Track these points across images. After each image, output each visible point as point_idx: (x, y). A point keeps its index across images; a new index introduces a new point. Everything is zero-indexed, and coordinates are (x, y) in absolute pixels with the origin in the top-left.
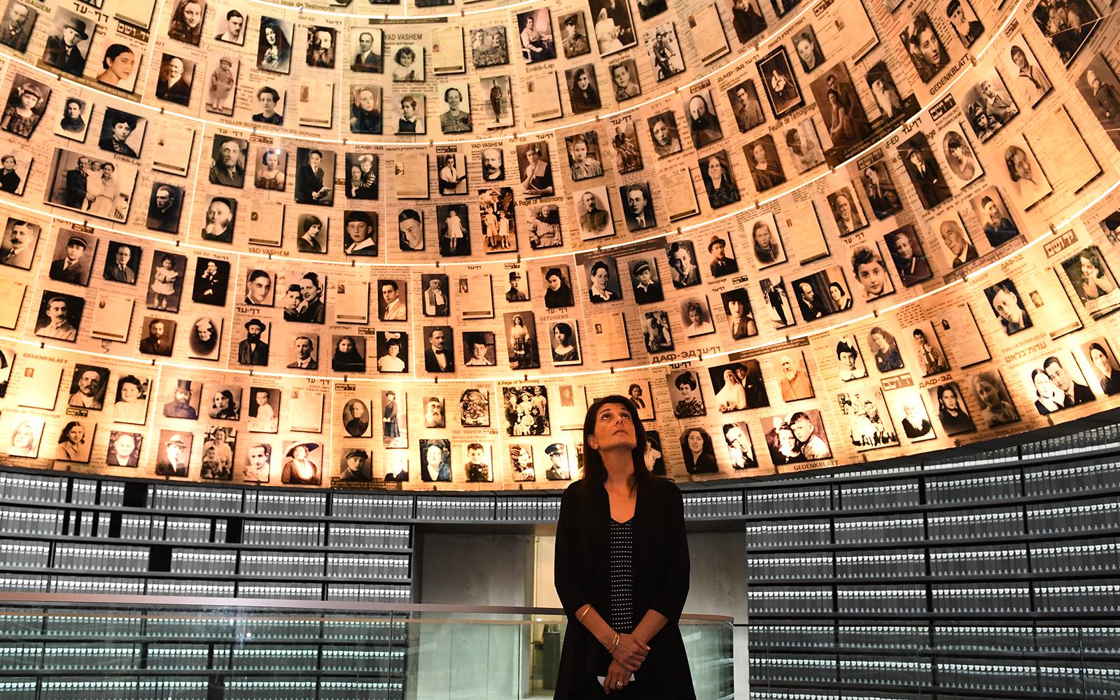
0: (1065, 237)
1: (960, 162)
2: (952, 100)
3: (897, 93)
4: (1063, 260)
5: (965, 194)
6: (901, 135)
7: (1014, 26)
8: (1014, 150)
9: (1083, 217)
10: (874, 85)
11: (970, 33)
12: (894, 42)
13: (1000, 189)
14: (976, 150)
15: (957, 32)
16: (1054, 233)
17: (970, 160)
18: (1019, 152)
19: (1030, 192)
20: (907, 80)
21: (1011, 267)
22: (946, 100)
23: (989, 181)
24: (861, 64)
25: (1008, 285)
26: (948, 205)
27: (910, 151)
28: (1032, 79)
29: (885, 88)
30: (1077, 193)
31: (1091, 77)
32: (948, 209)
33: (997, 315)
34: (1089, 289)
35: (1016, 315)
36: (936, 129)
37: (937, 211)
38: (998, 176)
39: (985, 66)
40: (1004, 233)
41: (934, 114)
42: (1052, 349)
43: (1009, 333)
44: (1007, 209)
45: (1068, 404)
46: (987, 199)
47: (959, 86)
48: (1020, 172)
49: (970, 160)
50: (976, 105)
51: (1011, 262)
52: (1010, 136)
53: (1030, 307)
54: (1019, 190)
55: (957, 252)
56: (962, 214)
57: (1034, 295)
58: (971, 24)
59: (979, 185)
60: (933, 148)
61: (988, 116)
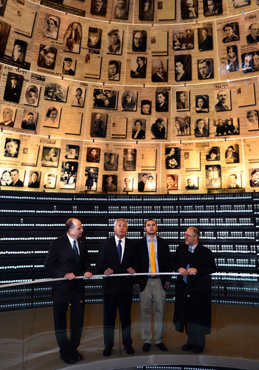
0: (51, 141)
1: (31, 97)
2: (44, 80)
3: (24, 57)
4: (45, 146)
5: (24, 106)
6: (14, 69)
7: (85, 85)
8: (54, 109)
9: (62, 139)
10: (17, 46)
11: (68, 71)
12: (37, 44)
13: (40, 115)
14: (40, 99)
15: (64, 66)
16: (49, 138)
17: (35, 99)
18: (56, 111)
19: (49, 122)
20: (32, 57)
21: (23, 137)
22: (42, 77)
23: (37, 110)
24: (17, 34)
25: (18, 142)
26: (14, 104)
27: (13, 77)
28: (78, 100)
29: (20, 51)
30: (66, 134)
31: (98, 116)
32: (14, 106)
33: (5, 148)
34: (47, 157)
35: (13, 151)
36: (30, 81)
37: (8, 103)
38: (42, 111)
39: (64, 83)
40: (29, 126)
41: (33, 76)
42: (19, 167)
43: (5, 155)
44: (37, 121)
45: (11, 185)
46: (32, 114)
47: (52, 78)
48: (51, 115)
49: (35, 99)
50: (52, 88)
51: (25, 136)
52: (58, 105)
53: (21, 151)
54: (46, 120)
55: (6, 121)
56: (18, 111)
57: (26, 149)
58: (71, 70)
59: (33, 108)
60: (24, 85)
61: (52, 93)
